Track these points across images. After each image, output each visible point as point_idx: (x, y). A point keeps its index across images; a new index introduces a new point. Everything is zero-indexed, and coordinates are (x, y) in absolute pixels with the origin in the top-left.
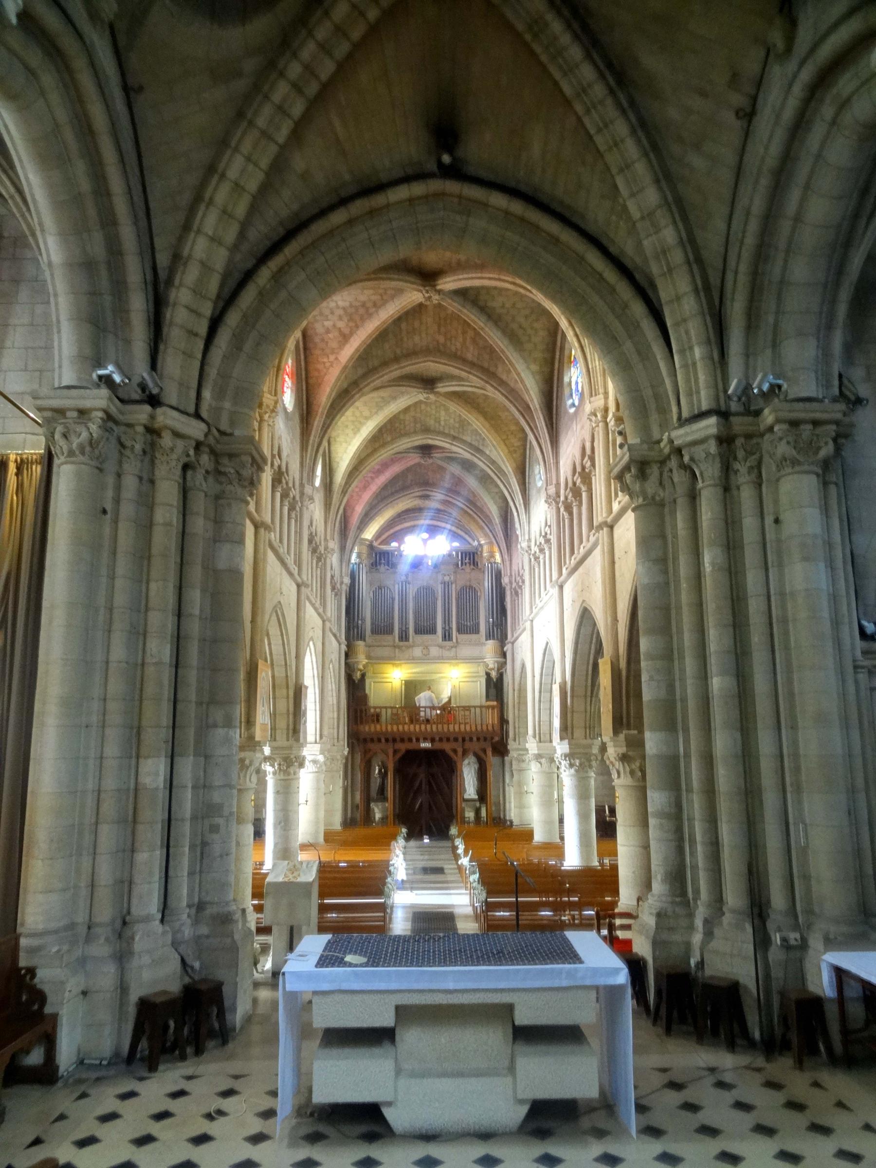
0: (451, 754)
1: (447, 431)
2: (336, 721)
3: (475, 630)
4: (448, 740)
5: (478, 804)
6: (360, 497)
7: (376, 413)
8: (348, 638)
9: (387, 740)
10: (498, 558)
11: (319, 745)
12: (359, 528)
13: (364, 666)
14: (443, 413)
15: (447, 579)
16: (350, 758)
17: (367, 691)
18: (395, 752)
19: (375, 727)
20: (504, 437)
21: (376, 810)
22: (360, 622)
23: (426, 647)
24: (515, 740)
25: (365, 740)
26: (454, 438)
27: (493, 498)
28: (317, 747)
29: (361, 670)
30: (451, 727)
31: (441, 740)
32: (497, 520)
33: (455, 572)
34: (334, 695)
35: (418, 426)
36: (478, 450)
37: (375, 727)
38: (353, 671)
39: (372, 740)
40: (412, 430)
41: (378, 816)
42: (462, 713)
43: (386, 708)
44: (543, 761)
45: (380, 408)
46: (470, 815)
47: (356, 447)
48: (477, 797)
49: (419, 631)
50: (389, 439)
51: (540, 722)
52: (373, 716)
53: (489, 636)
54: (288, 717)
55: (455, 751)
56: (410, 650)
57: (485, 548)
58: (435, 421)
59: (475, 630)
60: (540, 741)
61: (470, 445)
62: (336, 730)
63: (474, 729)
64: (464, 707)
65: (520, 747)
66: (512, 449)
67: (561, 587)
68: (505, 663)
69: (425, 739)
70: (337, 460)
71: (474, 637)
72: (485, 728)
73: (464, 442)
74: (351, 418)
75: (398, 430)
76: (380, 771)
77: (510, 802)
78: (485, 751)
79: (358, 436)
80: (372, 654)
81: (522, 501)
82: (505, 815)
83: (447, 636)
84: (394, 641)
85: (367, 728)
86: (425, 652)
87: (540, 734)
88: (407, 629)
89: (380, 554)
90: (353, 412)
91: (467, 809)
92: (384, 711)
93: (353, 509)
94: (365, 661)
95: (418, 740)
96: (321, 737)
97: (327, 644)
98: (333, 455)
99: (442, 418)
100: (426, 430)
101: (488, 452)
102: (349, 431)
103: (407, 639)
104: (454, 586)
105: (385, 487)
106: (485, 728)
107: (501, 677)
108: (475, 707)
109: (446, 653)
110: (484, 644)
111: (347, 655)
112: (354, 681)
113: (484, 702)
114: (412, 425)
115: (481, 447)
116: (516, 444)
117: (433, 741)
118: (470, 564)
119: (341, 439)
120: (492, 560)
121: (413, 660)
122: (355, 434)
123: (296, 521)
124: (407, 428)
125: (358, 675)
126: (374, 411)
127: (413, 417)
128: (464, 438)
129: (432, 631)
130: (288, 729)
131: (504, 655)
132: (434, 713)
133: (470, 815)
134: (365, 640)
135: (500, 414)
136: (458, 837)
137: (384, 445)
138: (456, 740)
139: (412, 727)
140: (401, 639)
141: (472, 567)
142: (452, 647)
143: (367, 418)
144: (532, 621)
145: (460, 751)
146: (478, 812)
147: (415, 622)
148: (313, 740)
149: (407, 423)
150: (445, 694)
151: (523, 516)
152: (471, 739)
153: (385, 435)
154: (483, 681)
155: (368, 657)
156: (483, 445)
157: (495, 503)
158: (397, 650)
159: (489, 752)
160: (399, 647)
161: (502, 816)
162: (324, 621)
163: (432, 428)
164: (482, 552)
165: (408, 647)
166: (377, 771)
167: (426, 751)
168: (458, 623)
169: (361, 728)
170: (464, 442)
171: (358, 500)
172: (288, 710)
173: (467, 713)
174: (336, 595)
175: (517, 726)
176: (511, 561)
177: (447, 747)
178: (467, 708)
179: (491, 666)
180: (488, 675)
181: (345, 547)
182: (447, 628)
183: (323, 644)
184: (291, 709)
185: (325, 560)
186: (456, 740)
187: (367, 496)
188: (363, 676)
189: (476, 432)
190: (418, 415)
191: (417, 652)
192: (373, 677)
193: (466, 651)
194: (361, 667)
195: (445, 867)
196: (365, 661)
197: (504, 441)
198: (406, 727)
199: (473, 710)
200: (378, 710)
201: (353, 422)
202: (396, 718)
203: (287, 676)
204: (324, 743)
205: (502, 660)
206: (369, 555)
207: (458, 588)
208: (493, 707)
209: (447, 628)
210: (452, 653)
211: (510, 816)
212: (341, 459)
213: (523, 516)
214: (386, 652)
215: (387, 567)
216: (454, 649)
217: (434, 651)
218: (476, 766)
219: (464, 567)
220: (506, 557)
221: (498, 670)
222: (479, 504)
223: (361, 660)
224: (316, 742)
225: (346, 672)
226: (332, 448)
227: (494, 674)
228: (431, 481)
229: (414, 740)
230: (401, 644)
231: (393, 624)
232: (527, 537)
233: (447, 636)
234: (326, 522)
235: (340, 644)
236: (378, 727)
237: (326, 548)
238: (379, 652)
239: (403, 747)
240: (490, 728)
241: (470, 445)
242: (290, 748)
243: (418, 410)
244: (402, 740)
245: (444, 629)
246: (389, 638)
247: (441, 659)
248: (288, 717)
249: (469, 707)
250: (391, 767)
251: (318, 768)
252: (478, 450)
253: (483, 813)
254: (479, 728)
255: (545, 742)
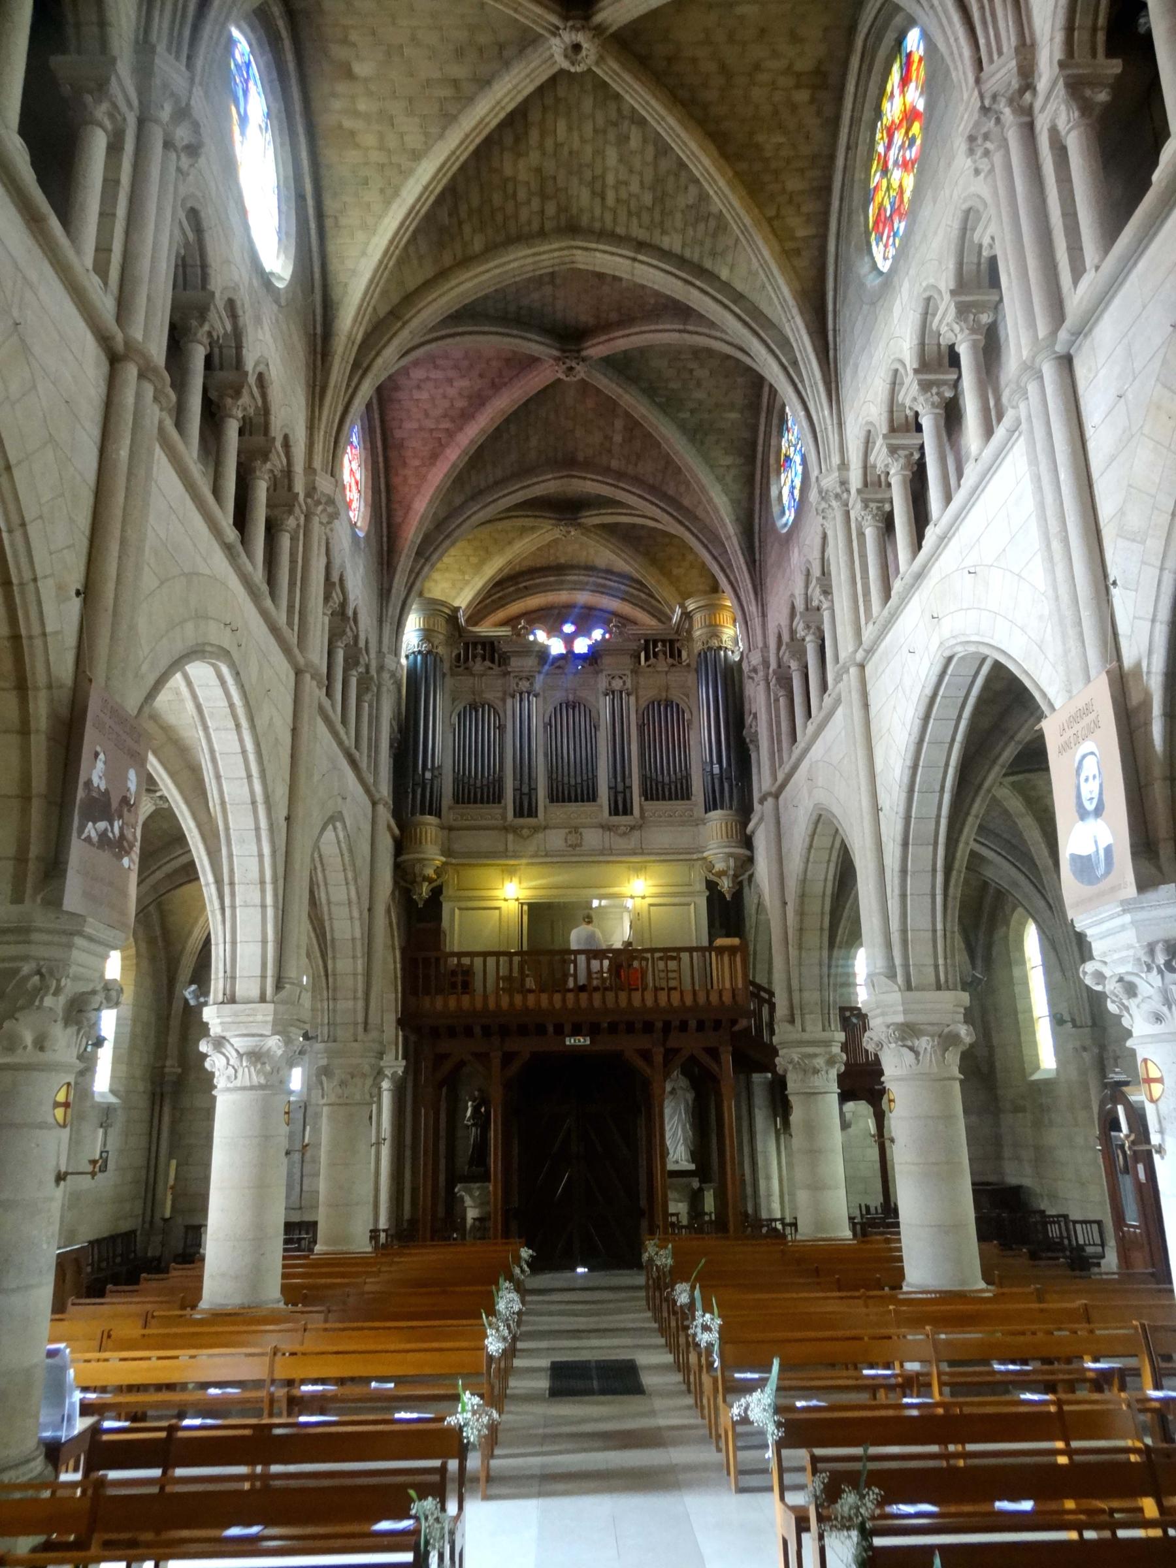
0: (639, 1063)
1: (620, 230)
2: (360, 979)
3: (682, 792)
4: (630, 1028)
5: (695, 1184)
6: (423, 478)
7: (441, 136)
8: (398, 813)
9: (487, 1031)
10: (730, 633)
11: (271, 1007)
12: (417, 553)
13: (439, 871)
14: (612, 155)
15: (617, 684)
16: (410, 1078)
17: (445, 924)
18: (508, 1058)
19: (458, 1001)
20: (771, 212)
21: (468, 1201)
22: (428, 775)
23: (576, 830)
24: (792, 1021)
25: (435, 1032)
26: (641, 246)
27: (720, 479)
28: (265, 1013)
29: (431, 881)
30: (636, 998)
31: (613, 1028)
32: (729, 530)
33: (635, 672)
34: (356, 914)
35: (551, 209)
36: (701, 272)
37: (458, 1001)
38: (414, 882)
39: (452, 1032)
40: (535, 226)
41: (472, 1214)
42: (661, 964)
43: (485, 955)
44: (923, 1043)
45: (448, 119)
46: (679, 1208)
47: (389, 235)
48: (692, 1167)
49: (558, 795)
50: (478, 245)
51: (904, 931)
52: (453, 973)
53: (712, 804)
54: (25, 812)
55: (646, 1055)
56: (540, 835)
57: (698, 618)
58: (593, 193)
59: (682, 792)
60: (909, 987)
61: (681, 261)
62: (360, 1004)
63: (689, 1001)
64: (665, 950)
65: (806, 1036)
66: (790, 245)
67: (1067, 362)
68: (751, 860)
69: (576, 1032)
70: (342, 278)
71: (679, 806)
72: (714, 998)
73: (665, 254)
74: (376, 156)
75: (499, 218)
76: (476, 1110)
77: (768, 1178)
78: (713, 1053)
79: (394, 206)
80: (456, 847)
81: (818, 375)
82: (757, 1207)
83: (621, 806)
84: (504, 817)
85: (439, 1003)
86: (572, 839)
87: (906, 966)
88: (533, 790)
89: (475, 644)
90: (381, 136)
91: (671, 1195)
92: (478, 961)
93: (408, 508)
94: (439, 860)
95: (560, 1031)
96: (279, 986)
97: (305, 730)
98: (334, 265)
99: (610, 179)
100: (572, 229)
101: (724, 274)
102: (372, 196)
103: (532, 813)
104: (632, 699)
105: (478, 458)
106: (714, 998)
107: (738, 895)
108: (690, 950)
109: (621, 843)
110: (703, 822)
111: (400, 847)
112: (415, 903)
113: (705, 942)
114: (535, 203)
115: (708, 264)
116: (801, 233)
117: (593, 1030)
118: (665, 653)
119: (352, 218)
120: (715, 643)
121: (547, 858)
122: (388, 203)
123: (115, 148)
124: (524, 214)
125: (425, 890)
126: (434, 130)
127: (538, 170)
128: (666, 242)
129: (588, 795)
130: (21, 859)
131: (747, 842)
132: (595, 964)
133: (679, 1208)
134: (440, 817)
135: (760, 138)
136: (679, 1273)
137: (466, 261)
138: (648, 1027)
139: (544, 998)
140: (519, 812)
141: (670, 661)
142: (632, 828)
143: (417, 156)
144: (862, 667)
145: (659, 1059)
146: (695, 1200)
147: (550, 778)
148: (255, 993)
149: (522, 195)
150: (620, 934)
151: (822, 413)
152: (683, 1027)
153: (467, 229)
154: (702, 902)
155: (447, 852)
156: (713, 254)
157: (726, 492)
158: (511, 837)
159: (728, 1060)
160: (515, 830)
161: (750, 1211)
162: (298, 673)
163: (585, 221)
164: (689, 631)
165: (535, 829)
166: (469, 1113)
167: (577, 1054)
168: (644, 778)
169: (427, 1002)
170: (665, 254)
171: (418, 487)
172: (26, 779)
173: (672, 965)
174: (364, 685)
175: (795, 984)
176: (764, 615)
177: (628, 1045)
178: (671, 953)
179: (720, 866)
180: (711, 886)
181: (389, 591)
182: (620, 787)
183: (295, 731)
184: (39, 782)
185: (308, 517)
186: (648, 1027)
187: (438, 475)
188: (437, 892)
189: (700, 212)
190: (550, 166)
191: (556, 839)
192: (460, 899)
193: (661, 837)
194: (430, 872)
195: (643, 1359)
196: (439, 860)
197: (770, 220)
198: (531, 998)
199: (685, 956)
200: (466, 961)
201: (382, 167)
202: (512, 985)
203: (16, 638)
204: (284, 1002)
205: (748, 853)
206: (451, 641)
207: (643, 704)
208: (732, 950)
209: (620, 787)
210: (634, 839)
211: (769, 1210)
212: (354, 272)
213: (822, 413)
214: (485, 841)
215: (488, 663)
216: (637, 833)
217: (593, 838)
218: (690, 1096)
219: (652, 660)
220: (753, 609)
221: (735, 876)
222: (686, 502)
223: (431, 856)
224: (263, 999)
225: (396, 883)
226: (331, 248)
227: (725, 884)
228: (580, 457)
229: (551, 1029)
230: (521, 821)
231: (501, 780)
232: (836, 460)
233: (621, 806)
234: (311, 428)
235: (374, 804)
236: (466, 999)
237: (311, 490)
238: (466, 841)
239: (526, 1047)
240: (727, 998)
241: (681, 261)
242: (22, 931)
243: (549, 144)
244: (523, 1031)
245: (613, 789)
246: (495, 810)
247: (606, 855)
248: (25, 812)
249: (679, 950)
250: (496, 1094)
251: (267, 1076)
252: (701, 272)
253: (709, 1203)
254: (702, 999)
255: (921, 988)
